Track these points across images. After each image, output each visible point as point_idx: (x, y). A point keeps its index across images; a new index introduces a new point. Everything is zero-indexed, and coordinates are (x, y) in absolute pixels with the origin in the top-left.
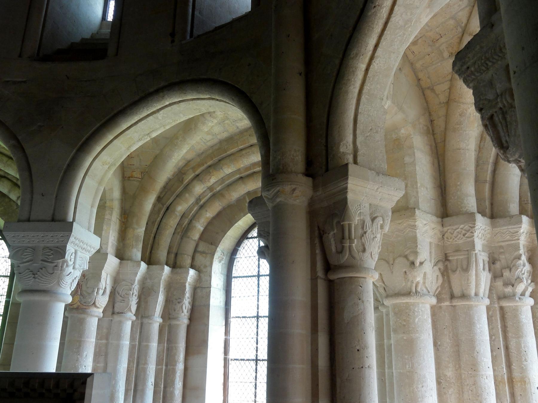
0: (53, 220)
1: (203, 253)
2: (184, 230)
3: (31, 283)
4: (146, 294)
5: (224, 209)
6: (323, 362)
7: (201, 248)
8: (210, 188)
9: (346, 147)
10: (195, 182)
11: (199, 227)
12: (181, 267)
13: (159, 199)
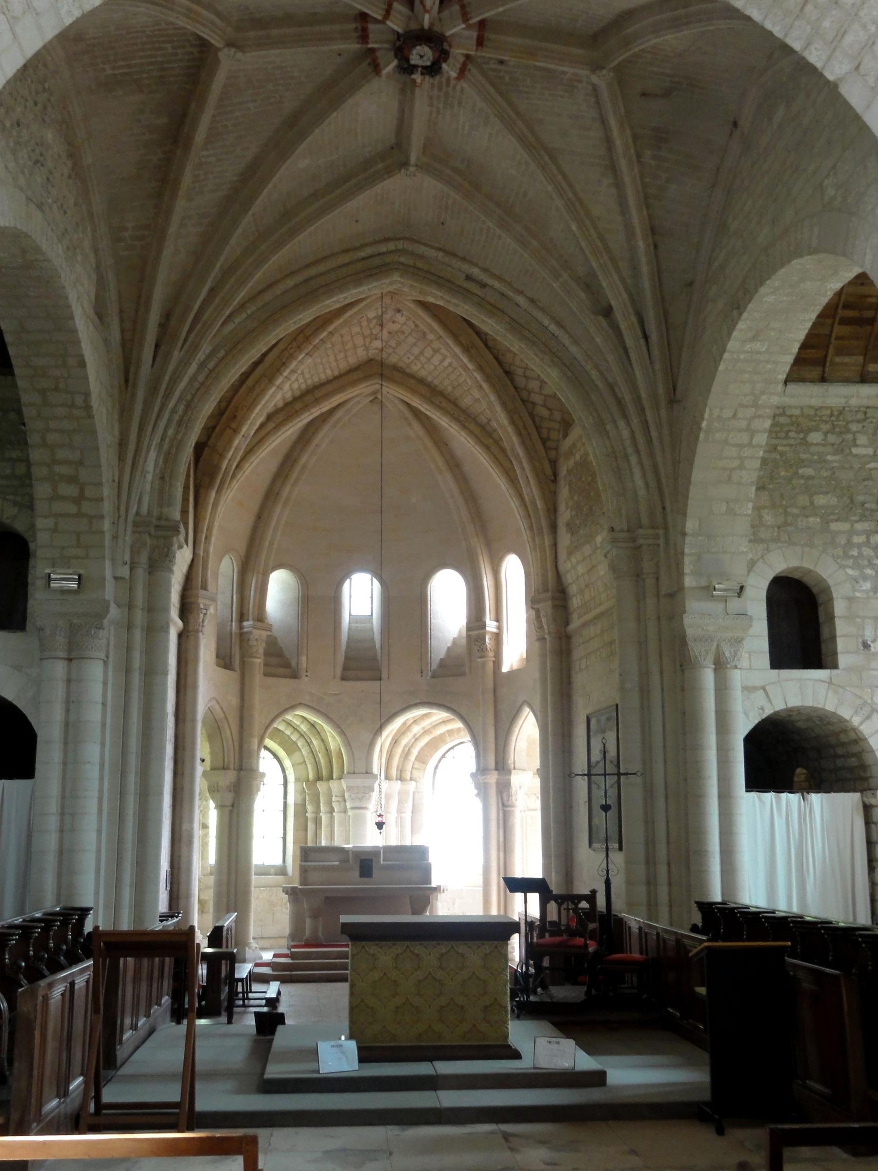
1: (418, 769)
2: (406, 755)
3: (358, 804)
5: (431, 740)
6: (501, 839)
7: (416, 766)
8: (423, 728)
9: (511, 761)
11: (415, 752)
12: (406, 780)
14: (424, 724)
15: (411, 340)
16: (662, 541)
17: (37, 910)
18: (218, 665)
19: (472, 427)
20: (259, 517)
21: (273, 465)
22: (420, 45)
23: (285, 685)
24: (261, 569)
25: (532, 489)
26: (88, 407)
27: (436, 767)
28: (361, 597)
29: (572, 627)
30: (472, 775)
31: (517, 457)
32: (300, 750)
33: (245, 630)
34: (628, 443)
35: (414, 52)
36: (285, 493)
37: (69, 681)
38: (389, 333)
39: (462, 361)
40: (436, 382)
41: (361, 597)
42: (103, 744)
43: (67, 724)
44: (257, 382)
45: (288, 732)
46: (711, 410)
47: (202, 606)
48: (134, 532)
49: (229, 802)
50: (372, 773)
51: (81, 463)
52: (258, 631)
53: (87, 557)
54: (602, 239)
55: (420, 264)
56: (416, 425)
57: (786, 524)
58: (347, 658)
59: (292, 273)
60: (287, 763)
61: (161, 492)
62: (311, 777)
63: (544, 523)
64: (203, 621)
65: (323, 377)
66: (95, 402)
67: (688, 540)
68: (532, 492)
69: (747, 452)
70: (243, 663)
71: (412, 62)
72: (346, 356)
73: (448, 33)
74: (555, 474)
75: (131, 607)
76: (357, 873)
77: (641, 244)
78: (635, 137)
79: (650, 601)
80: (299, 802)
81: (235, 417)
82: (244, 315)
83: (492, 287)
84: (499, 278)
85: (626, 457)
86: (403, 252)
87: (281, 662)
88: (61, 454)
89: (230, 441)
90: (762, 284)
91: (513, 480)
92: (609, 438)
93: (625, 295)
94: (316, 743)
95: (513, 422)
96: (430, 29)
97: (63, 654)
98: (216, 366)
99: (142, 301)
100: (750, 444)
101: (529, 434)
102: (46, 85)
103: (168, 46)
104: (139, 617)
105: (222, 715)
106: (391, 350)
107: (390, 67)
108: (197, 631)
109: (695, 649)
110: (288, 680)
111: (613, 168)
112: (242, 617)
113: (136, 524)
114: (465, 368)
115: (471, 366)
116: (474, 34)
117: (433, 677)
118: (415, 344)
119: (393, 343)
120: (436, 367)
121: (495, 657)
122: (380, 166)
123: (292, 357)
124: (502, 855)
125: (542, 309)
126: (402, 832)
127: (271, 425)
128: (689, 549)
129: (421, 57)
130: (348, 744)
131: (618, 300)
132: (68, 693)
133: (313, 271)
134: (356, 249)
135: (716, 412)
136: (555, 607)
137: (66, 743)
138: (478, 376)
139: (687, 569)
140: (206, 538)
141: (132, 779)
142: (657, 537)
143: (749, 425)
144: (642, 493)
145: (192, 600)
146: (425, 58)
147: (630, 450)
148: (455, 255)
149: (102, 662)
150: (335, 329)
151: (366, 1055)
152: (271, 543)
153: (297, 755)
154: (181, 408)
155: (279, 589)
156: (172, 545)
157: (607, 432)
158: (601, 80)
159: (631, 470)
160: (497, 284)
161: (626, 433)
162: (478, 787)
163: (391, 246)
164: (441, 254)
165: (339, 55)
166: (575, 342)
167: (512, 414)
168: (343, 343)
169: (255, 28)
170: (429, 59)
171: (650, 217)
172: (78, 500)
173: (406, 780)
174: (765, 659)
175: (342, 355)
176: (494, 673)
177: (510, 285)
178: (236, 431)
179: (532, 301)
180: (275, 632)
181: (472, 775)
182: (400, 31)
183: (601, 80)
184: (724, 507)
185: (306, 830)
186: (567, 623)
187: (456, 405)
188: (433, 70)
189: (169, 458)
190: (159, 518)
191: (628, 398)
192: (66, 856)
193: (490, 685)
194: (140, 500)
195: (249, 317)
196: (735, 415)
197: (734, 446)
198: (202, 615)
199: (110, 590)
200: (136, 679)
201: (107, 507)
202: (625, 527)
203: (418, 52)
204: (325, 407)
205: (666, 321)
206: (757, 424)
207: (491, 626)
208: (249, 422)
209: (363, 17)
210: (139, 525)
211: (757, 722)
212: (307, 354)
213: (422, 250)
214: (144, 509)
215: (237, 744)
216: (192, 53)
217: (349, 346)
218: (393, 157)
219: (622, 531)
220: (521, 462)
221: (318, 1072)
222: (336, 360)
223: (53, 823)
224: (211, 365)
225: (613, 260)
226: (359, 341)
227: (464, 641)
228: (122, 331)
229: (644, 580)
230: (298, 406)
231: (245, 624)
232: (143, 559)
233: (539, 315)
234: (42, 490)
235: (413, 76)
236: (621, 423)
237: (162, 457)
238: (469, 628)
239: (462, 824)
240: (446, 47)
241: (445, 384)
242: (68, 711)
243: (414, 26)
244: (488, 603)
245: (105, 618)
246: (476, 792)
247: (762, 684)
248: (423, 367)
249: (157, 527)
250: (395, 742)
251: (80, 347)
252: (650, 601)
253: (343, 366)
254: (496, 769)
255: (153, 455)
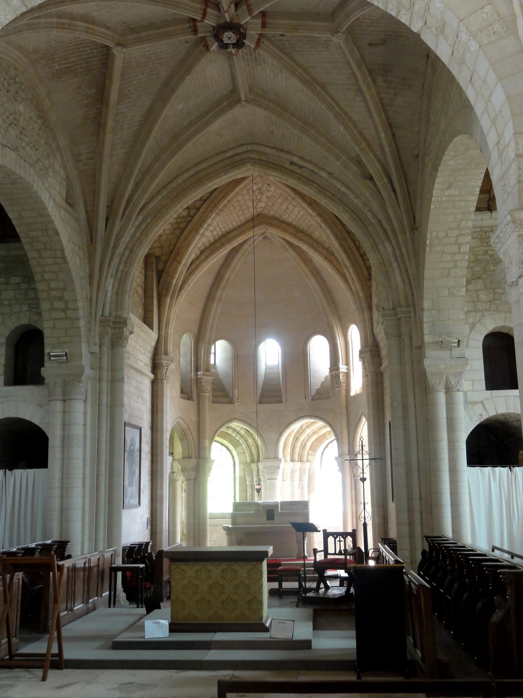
0: (275, 458)
1: (311, 455)
2: (303, 447)
3: (271, 477)
4: (293, 472)
6: (354, 496)
7: (310, 453)
8: (313, 430)
10: (307, 429)
11: (309, 444)
12: (304, 462)
13: (294, 437)
14: (310, 429)
15: (280, 201)
16: (412, 315)
17: (32, 542)
18: (182, 398)
19: (320, 249)
20: (204, 310)
21: (210, 280)
22: (227, 32)
23: (226, 408)
24: (207, 339)
25: (357, 285)
26: (64, 258)
27: (323, 453)
28: (270, 354)
29: (382, 367)
30: (336, 458)
31: (346, 266)
32: (241, 445)
33: (199, 377)
34: (391, 255)
35: (224, 36)
36: (218, 296)
37: (64, 412)
38: (267, 197)
39: (308, 211)
40: (298, 224)
41: (270, 354)
42: (85, 448)
43: (63, 437)
44: (190, 232)
45: (234, 435)
46: (430, 233)
47: (165, 365)
48: (101, 326)
49: (193, 477)
50: (278, 458)
51: (64, 289)
52: (207, 377)
53: (72, 342)
54: (361, 134)
55: (263, 158)
56: (291, 251)
57: (494, 299)
58: (263, 390)
59: (187, 170)
60: (235, 453)
61: (117, 301)
62: (248, 461)
63: (364, 306)
64: (166, 373)
65: (231, 226)
66: (68, 253)
67: (425, 313)
68: (356, 287)
69: (457, 257)
70: (199, 396)
71: (225, 42)
72: (244, 214)
73: (243, 22)
74: (370, 275)
75: (100, 368)
76: (266, 518)
77: (383, 135)
78: (370, 71)
79: (407, 352)
80: (242, 475)
81: (179, 254)
82: (160, 197)
83: (306, 167)
84: (310, 162)
85: (391, 264)
86: (252, 151)
87: (223, 394)
88: (53, 285)
89: (176, 269)
90: (443, 154)
91: (346, 280)
92: (380, 253)
93: (378, 166)
94: (250, 441)
95: (341, 246)
96: (231, 22)
97: (60, 397)
98: (146, 227)
99: (96, 194)
100: (459, 252)
101: (352, 252)
102: (17, 80)
103: (88, 49)
104: (105, 374)
105: (186, 427)
106: (270, 208)
107: (215, 46)
108: (163, 379)
109: (432, 380)
110: (227, 405)
111: (360, 90)
112: (197, 369)
113: (101, 322)
114: (311, 216)
115: (314, 214)
116: (259, 21)
117: (313, 400)
118: (282, 204)
119: (270, 203)
120: (296, 216)
121: (346, 387)
122: (226, 103)
123: (207, 217)
124: (354, 505)
125: (336, 178)
126: (302, 493)
127: (203, 257)
128: (427, 317)
129: (229, 38)
130: (264, 441)
131: (374, 169)
132: (64, 420)
133: (200, 167)
134: (223, 152)
135: (434, 234)
136: (372, 355)
137: (63, 447)
138: (318, 220)
139: (426, 331)
140: (166, 325)
141: (103, 468)
142: (409, 312)
143: (456, 240)
144: (401, 285)
145: (158, 361)
146: (232, 39)
147: (393, 260)
148: (282, 150)
149: (82, 402)
150: (231, 198)
151: (173, 628)
152: (212, 326)
153: (240, 448)
154: (127, 253)
155: (220, 353)
156: (123, 332)
157: (379, 250)
158: (338, 39)
159: (394, 272)
160: (308, 166)
161: (390, 249)
162: (339, 465)
163: (245, 148)
164: (274, 150)
165: (187, 42)
166: (357, 196)
167: (340, 240)
168: (240, 205)
169: (135, 32)
170: (234, 39)
171: (388, 118)
172: (65, 310)
173: (304, 462)
174: (483, 384)
175: (241, 212)
176: (346, 396)
177: (316, 165)
178: (179, 262)
179: (330, 174)
180: (221, 377)
181: (336, 458)
182: (214, 25)
183: (338, 39)
184: (447, 292)
185: (247, 492)
186: (381, 365)
187: (311, 237)
188: (239, 45)
189: (121, 282)
190: (116, 317)
191: (388, 228)
192: (64, 510)
193: (344, 404)
194: (104, 307)
195: (163, 197)
196: (446, 236)
197: (449, 254)
198: (165, 370)
199: (86, 361)
200: (104, 410)
201: (81, 313)
202: (391, 307)
203: (229, 35)
204: (235, 244)
205: (406, 180)
206: (461, 239)
207: (343, 368)
208: (187, 256)
209: (194, 20)
210: (104, 322)
211: (478, 424)
212: (217, 214)
213: (263, 149)
214: (107, 313)
215: (196, 443)
216: (102, 51)
217: (244, 207)
218: (231, 98)
219: (389, 309)
220: (348, 269)
221: (144, 637)
222: (238, 216)
223: (57, 493)
224: (143, 227)
225: (369, 145)
226: (250, 204)
227: (329, 379)
228: (87, 212)
229: (403, 339)
230: (218, 245)
231: (199, 373)
232: (107, 341)
233: (334, 182)
234: (45, 306)
235: (229, 50)
236: (387, 244)
237: (117, 282)
238: (331, 370)
239: (326, 488)
240: (242, 31)
241: (304, 226)
242: (64, 429)
243: (222, 21)
244: (341, 355)
245: (81, 376)
246: (338, 468)
247: (481, 400)
248: (289, 216)
249: (114, 322)
250: (296, 439)
251: (54, 225)
252: (407, 352)
253: (243, 219)
254: (349, 454)
255: (110, 281)
